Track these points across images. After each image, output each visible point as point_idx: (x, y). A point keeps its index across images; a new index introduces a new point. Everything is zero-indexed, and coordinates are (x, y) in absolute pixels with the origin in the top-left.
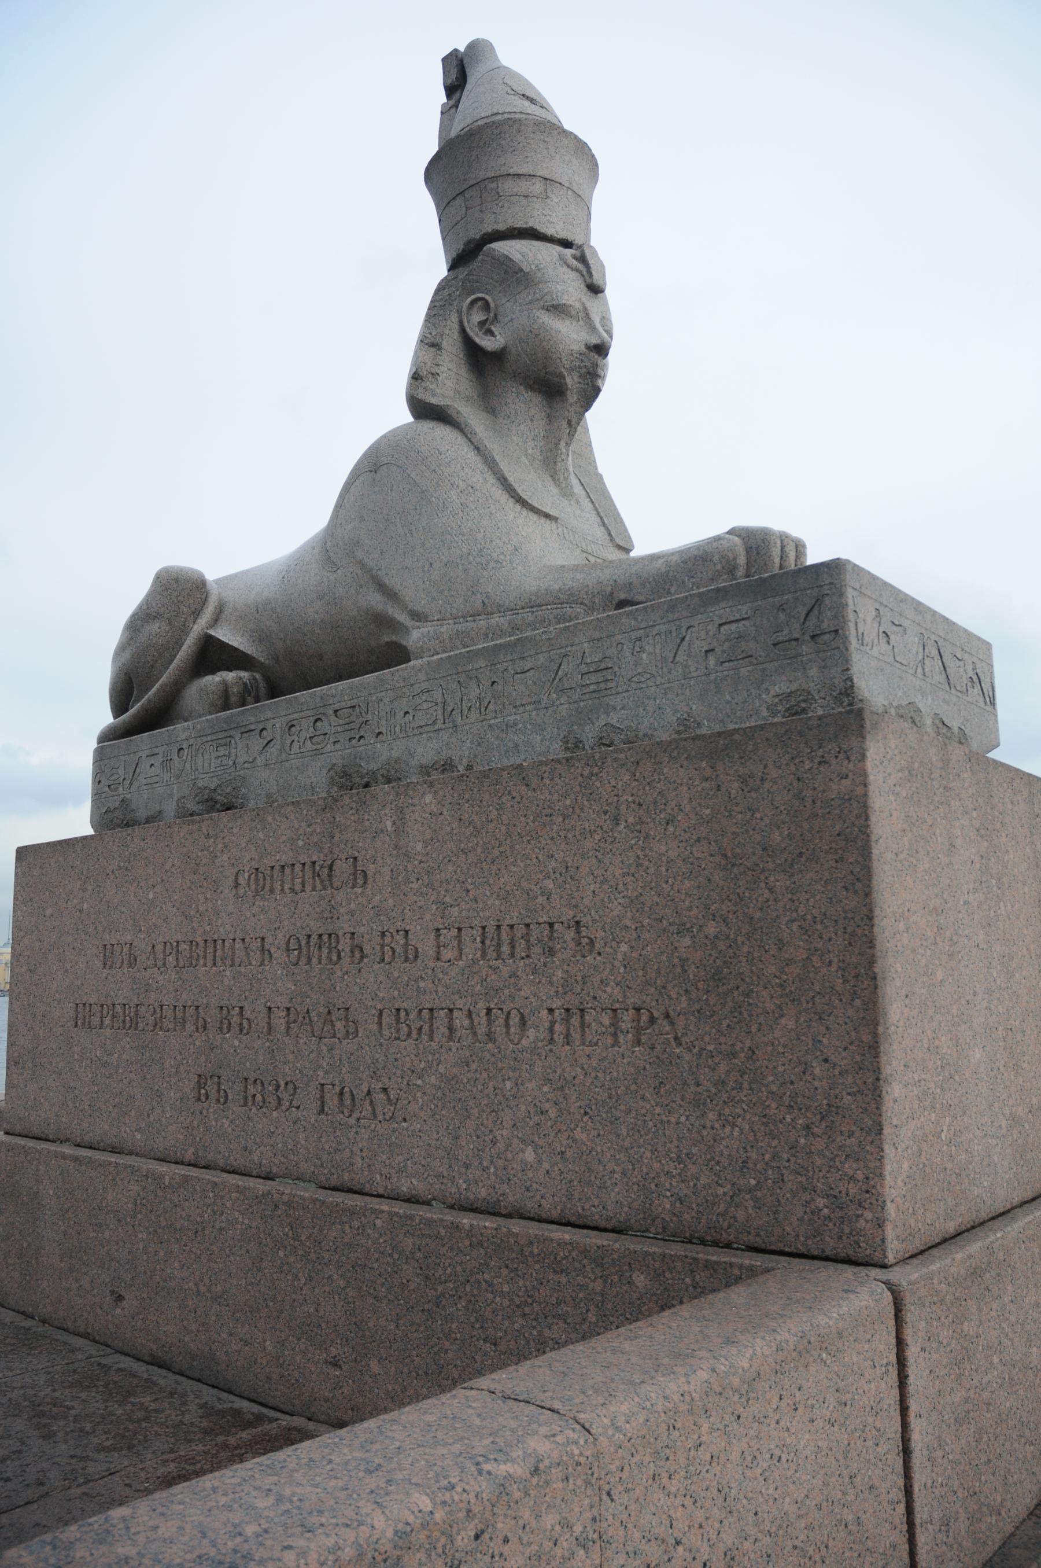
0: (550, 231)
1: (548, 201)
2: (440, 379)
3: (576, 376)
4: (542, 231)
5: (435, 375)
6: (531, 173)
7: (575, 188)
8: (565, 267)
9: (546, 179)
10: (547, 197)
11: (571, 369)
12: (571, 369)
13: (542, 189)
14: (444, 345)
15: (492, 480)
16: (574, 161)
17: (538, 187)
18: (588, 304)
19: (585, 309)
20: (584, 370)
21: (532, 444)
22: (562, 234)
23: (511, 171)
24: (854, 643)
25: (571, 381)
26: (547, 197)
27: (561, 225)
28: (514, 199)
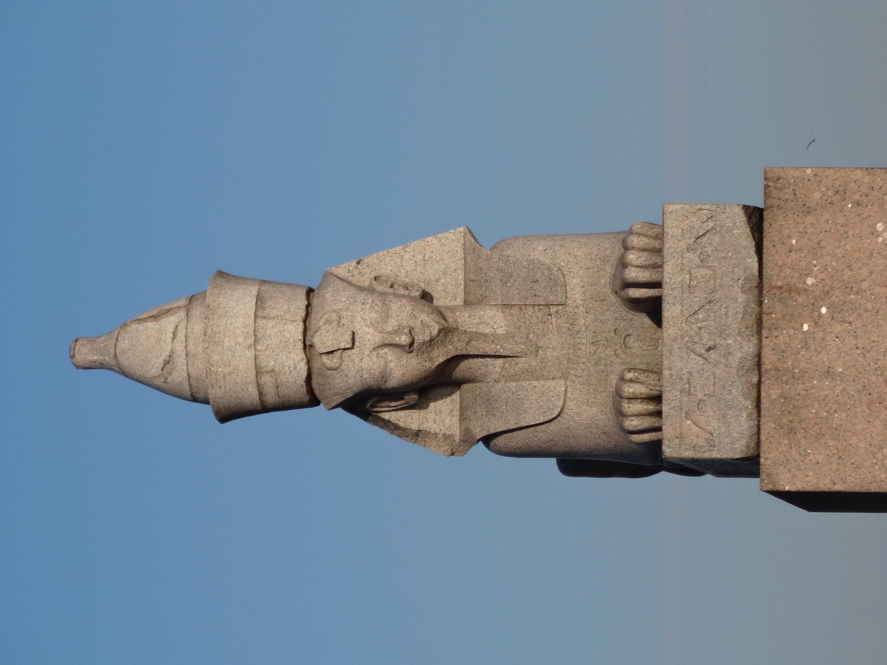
0: (303, 367)
1: (277, 369)
2: (448, 433)
3: (436, 352)
4: (305, 374)
5: (446, 437)
6: (255, 385)
7: (251, 341)
8: (342, 367)
9: (257, 372)
10: (273, 371)
11: (431, 360)
12: (431, 360)
13: (268, 376)
14: (415, 427)
15: (543, 427)
16: (227, 344)
17: (267, 380)
18: (369, 347)
19: (375, 349)
20: (429, 349)
21: (491, 368)
22: (302, 355)
23: (257, 398)
24: (715, 455)
25: (439, 357)
26: (273, 371)
27: (293, 355)
28: (281, 394)
